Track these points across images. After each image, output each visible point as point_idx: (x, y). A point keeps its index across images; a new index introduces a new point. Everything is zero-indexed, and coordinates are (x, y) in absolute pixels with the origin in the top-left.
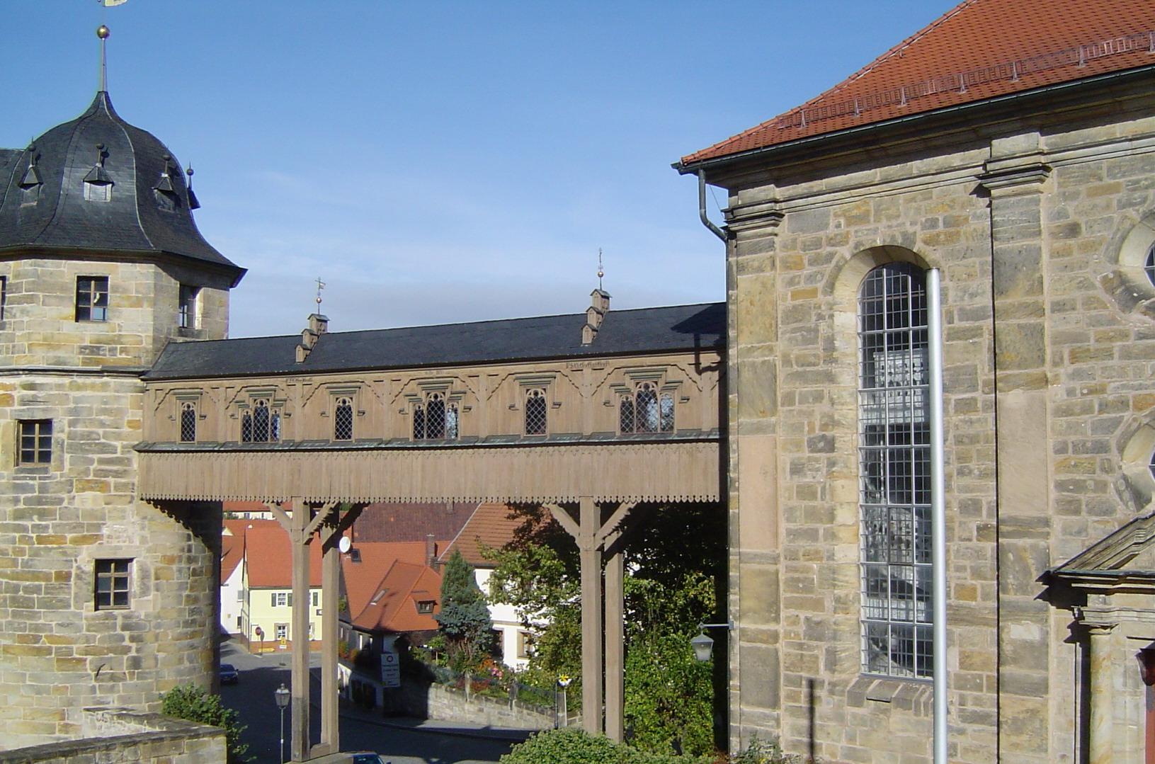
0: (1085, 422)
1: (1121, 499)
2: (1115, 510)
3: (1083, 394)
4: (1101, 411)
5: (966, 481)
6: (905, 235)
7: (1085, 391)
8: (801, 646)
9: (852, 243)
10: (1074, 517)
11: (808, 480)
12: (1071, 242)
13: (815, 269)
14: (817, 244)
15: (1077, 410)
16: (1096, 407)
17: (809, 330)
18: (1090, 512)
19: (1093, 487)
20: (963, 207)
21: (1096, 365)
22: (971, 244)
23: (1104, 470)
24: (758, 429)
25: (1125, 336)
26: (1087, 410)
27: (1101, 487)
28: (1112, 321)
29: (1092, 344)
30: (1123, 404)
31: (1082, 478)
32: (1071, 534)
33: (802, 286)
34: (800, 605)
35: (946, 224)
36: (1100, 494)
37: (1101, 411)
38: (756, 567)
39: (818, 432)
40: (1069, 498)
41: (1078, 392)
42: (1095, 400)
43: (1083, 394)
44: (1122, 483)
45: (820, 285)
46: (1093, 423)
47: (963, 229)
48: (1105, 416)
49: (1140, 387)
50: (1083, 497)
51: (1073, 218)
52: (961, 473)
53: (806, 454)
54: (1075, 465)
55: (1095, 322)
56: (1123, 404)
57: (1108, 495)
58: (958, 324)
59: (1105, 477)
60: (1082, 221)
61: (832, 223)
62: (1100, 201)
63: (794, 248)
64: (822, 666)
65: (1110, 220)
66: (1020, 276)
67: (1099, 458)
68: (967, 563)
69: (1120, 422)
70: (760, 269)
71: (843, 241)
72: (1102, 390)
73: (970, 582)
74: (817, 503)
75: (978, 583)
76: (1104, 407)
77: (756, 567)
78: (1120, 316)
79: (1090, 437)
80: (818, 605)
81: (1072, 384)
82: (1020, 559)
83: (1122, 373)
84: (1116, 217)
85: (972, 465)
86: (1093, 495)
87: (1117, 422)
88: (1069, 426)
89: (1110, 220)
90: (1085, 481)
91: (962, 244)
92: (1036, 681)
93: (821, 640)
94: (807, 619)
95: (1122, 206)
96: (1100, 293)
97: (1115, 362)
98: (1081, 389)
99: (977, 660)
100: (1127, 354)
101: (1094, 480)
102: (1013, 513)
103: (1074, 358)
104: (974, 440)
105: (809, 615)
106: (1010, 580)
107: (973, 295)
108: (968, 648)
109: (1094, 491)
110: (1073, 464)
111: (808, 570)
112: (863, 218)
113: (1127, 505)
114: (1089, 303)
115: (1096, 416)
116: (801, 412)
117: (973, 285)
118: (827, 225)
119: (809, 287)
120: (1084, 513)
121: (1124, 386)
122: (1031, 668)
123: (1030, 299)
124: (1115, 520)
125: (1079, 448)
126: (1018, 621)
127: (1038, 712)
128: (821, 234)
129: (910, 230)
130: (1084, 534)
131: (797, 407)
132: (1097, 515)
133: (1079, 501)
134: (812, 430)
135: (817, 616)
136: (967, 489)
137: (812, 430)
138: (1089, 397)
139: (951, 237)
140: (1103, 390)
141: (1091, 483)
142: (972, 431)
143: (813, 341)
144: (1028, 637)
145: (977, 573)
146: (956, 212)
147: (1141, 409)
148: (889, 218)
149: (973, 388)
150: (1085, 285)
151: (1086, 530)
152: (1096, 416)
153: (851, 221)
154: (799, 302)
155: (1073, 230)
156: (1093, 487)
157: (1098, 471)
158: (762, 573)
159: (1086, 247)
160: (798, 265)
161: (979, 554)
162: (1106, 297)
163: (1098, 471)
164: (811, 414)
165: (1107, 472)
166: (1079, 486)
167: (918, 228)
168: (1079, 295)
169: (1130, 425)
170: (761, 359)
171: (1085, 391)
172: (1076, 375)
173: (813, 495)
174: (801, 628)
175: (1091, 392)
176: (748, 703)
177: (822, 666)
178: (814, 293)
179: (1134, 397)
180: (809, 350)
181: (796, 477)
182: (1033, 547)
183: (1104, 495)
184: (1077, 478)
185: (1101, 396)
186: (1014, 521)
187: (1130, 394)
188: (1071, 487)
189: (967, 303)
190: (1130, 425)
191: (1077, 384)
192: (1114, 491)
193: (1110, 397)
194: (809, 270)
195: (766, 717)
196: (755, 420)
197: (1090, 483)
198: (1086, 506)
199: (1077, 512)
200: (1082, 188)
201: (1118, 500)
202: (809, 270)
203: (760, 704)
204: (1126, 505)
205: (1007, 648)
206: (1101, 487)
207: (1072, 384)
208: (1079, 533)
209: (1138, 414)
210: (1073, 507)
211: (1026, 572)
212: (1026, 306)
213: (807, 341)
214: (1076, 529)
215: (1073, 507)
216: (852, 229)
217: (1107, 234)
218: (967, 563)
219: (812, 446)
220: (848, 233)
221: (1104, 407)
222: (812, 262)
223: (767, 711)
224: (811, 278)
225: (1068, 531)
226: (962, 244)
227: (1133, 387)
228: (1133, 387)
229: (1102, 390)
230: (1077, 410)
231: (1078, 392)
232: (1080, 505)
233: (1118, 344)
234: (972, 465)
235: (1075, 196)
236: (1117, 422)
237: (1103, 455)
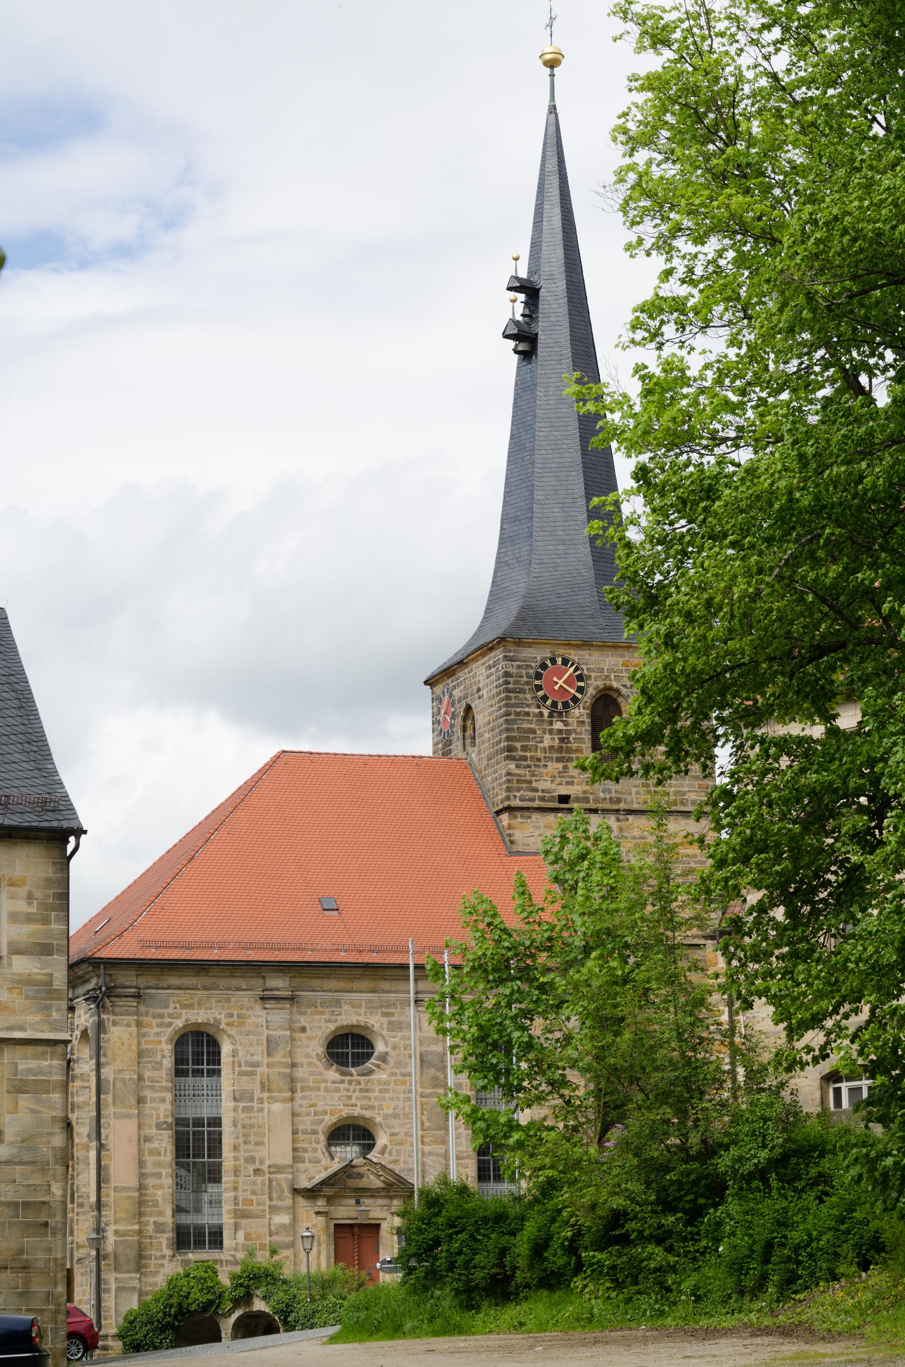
5: (248, 1147)
6: (215, 1019)
8: (151, 1237)
9: (184, 1017)
11: (156, 1145)
12: (302, 1035)
13: (160, 1030)
14: (162, 1016)
17: (156, 1063)
20: (248, 1009)
21: (313, 1094)
22: (252, 1029)
24: (127, 1116)
25: (326, 1081)
26: (308, 1114)
27: (315, 1150)
28: (320, 1074)
29: (311, 1084)
30: (325, 1113)
33: (152, 1038)
34: (151, 1215)
35: (238, 1017)
38: (126, 1194)
39: (162, 1119)
42: (312, 1110)
45: (164, 1039)
47: (248, 1020)
50: (307, 1155)
51: (303, 1024)
52: (245, 1142)
53: (154, 1131)
55: (312, 1074)
56: (325, 1113)
58: (243, 1068)
60: (307, 1026)
61: (172, 1005)
62: (317, 1017)
63: (147, 1016)
64: (164, 1247)
65: (320, 1027)
66: (280, 1048)
67: (314, 1137)
68: (248, 1188)
70: (128, 1025)
71: (179, 1017)
72: (315, 1105)
73: (251, 1197)
74: (162, 1158)
75: (254, 1198)
76: (316, 1114)
77: (126, 1194)
78: (324, 1072)
79: (310, 1127)
80: (161, 1214)
81: (301, 1102)
82: (279, 1184)
83: (325, 1098)
84: (324, 1026)
85: (251, 1139)
87: (322, 1121)
89: (320, 1027)
91: (247, 1028)
93: (163, 1232)
94: (155, 1222)
95: (327, 1021)
96: (314, 1060)
97: (322, 1093)
99: (254, 1236)
100: (327, 1090)
102: (276, 1162)
103: (302, 1089)
104: (252, 1126)
105: (156, 1219)
106: (274, 1194)
107: (252, 1055)
108: (249, 1230)
111: (155, 1195)
112: (190, 1006)
114: (310, 1064)
115: (312, 1117)
116: (151, 1108)
117: (253, 1050)
118: (168, 1007)
119: (156, 1039)
123: (284, 1060)
125: (305, 1132)
126: (278, 1214)
128: (165, 1011)
129: (218, 1017)
131: (148, 1105)
134: (158, 1117)
135: (161, 1220)
136: (248, 1151)
137: (158, 1117)
139: (241, 1024)
142: (251, 1122)
143: (160, 1069)
144: (283, 1221)
145: (254, 1193)
146: (244, 1012)
148: (206, 1009)
149: (252, 1100)
150: (307, 1056)
152: (312, 1117)
153: (183, 1006)
154: (149, 1047)
155: (303, 1029)
158: (129, 1197)
159: (308, 1038)
160: (150, 1026)
161: (254, 1183)
162: (318, 1063)
164: (158, 1109)
166: (305, 1150)
167: (223, 1017)
168: (304, 1060)
170: (128, 1077)
172: (304, 1098)
173: (159, 1154)
174: (150, 1228)
176: (120, 1272)
177: (164, 1247)
178: (160, 1042)
180: (156, 1074)
181: (147, 1144)
182: (286, 1179)
186: (276, 1166)
187: (328, 1108)
189: (249, 1058)
191: (303, 1102)
193: (319, 1109)
194: (156, 1030)
195: (131, 1279)
196: (124, 1111)
199: (304, 1162)
200: (309, 1010)
202: (156, 1030)
203: (128, 1272)
205: (273, 1228)
206: (315, 1150)
207: (301, 1102)
211: (282, 1191)
212: (282, 1063)
213: (154, 1069)
216: (184, 1011)
217: (319, 1034)
218: (248, 1188)
219: (158, 1126)
220: (181, 1014)
221: (316, 1114)
222: (159, 1025)
223: (133, 1275)
224: (158, 1034)
226: (247, 1028)
229: (315, 1105)
233: (322, 1085)
234: (251, 1139)
235: (305, 1013)
236: (322, 1121)
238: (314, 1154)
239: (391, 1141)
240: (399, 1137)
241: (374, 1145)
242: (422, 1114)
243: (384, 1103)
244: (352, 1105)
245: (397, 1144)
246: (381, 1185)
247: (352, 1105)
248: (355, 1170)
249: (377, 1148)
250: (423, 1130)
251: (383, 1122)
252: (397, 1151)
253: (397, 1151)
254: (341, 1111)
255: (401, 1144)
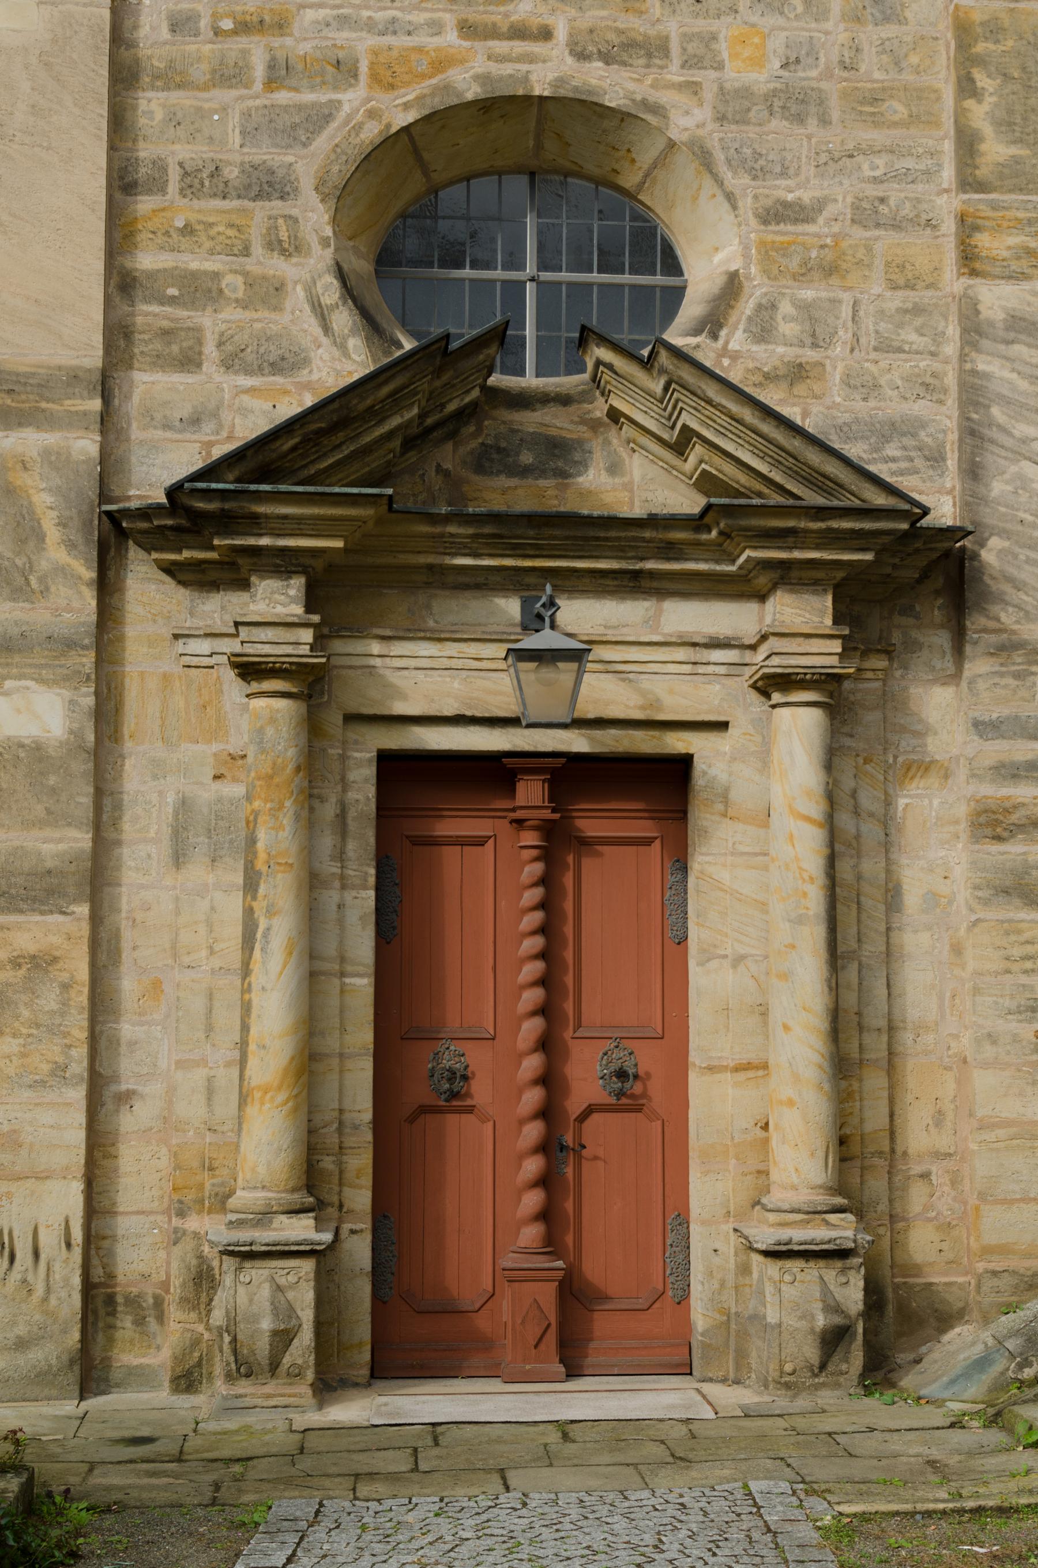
0: (224, 109)
1: (326, 329)
2: (306, 362)
3: (217, 32)
4: (272, 83)
7: (227, 24)
10: (178, 379)
15: (200, 72)
16: (259, 72)
18: (230, 362)
19: (240, 294)
23: (275, 245)
31: (210, 265)
32: (167, 426)
36: (264, 314)
37: (272, 83)
40: (165, 324)
41: (204, 23)
43: (217, 32)
44: (326, 288)
46: (247, 114)
48: (283, 97)
49: (391, 27)
54: (188, 230)
57: (285, 318)
59: (278, 266)
67: (261, 211)
69: (328, 118)
86: (231, 314)
87: (322, 117)
88: (174, 120)
90: (216, 276)
92: (49, 864)
98: (216, 16)
101: (246, 274)
109: (244, 305)
110: (180, 224)
113: (343, 347)
120: (210, 367)
121: (343, 21)
122: (29, 824)
124: (308, 386)
127: (55, 960)
130: (208, 427)
132: (248, 372)
133: (197, 331)
138: (242, 42)
140: (281, 26)
141: (239, 280)
147: (392, 87)
151: (215, 415)
156: (240, 294)
157: (258, 249)
163: (258, 249)
165: (284, 252)
169: (359, 127)
171: (227, 24)
175: (243, 27)
179: (375, 52)
182: (54, 459)
183: (274, 316)
184: (194, 265)
185: (277, 42)
188: (173, 291)
190: (359, 127)
192: (307, 308)
197: (233, 284)
198: (220, 344)
199: (190, 362)
201: (317, 331)
204: (343, 347)
208: (195, 421)
209: (383, 100)
210: (175, 348)
214: (185, 411)
215: (175, 348)
225: (158, 416)
227: (370, 26)
228: (370, 26)
229: (281, 26)
230: (200, 72)
231: (204, 23)
232: (200, 342)
236: (322, 117)
237: (277, 206)
238: (262, 319)
239: (769, 253)
240: (818, 227)
241: (675, 296)
242: (967, 88)
243: (726, 29)
244: (519, 32)
245: (803, 274)
246: (691, 503)
247: (519, 32)
248: (530, 420)
249: (691, 309)
250: (968, 182)
251: (714, 137)
252: (807, 310)
253: (805, 308)
254: (441, 63)
255: (831, 270)
